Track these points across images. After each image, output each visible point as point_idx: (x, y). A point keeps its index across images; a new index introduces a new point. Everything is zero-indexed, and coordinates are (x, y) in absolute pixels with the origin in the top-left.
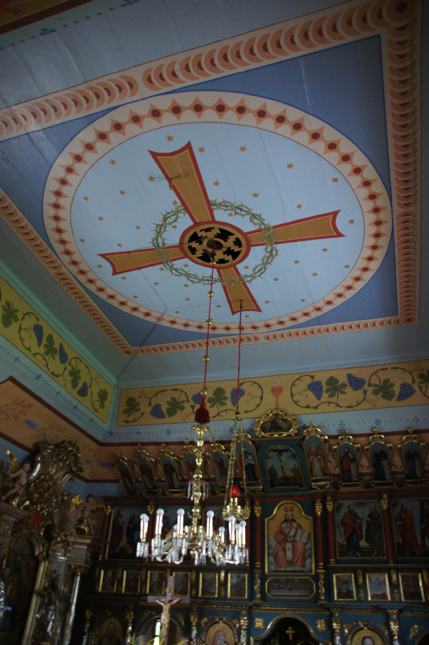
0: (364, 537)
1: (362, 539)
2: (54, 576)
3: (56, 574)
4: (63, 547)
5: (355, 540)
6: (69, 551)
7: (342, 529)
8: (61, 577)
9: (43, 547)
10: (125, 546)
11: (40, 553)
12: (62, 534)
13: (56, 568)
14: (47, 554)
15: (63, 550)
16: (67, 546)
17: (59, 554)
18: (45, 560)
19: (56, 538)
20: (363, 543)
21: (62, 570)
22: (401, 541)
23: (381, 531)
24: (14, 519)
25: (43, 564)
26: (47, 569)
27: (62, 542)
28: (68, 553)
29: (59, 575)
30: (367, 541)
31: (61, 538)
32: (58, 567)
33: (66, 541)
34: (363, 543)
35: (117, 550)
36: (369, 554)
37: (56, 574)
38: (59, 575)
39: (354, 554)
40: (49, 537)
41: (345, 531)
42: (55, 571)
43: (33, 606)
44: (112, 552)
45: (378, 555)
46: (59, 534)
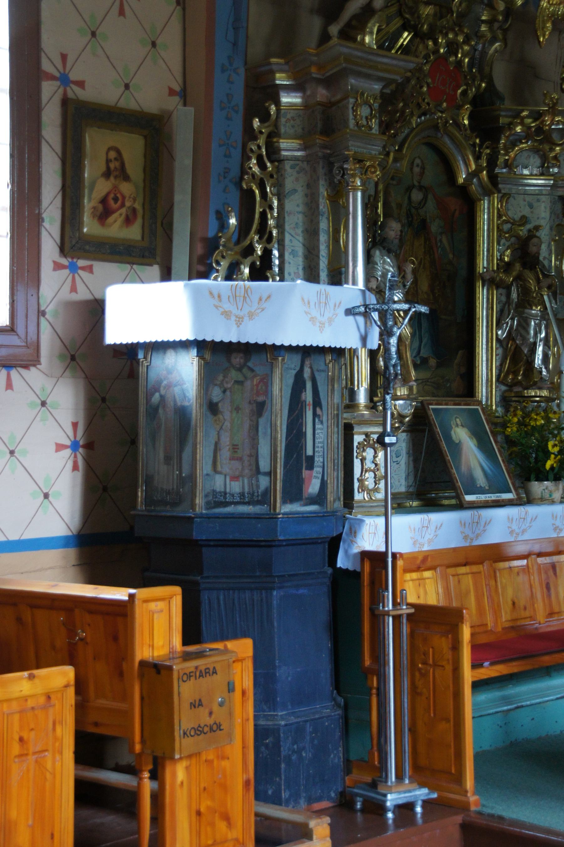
2: (523, 231)
3: (529, 226)
4: (535, 150)
6: (555, 158)
8: (544, 234)
9: (477, 158)
11: (471, 175)
12: (525, 113)
13: (526, 211)
14: (493, 178)
15: (536, 160)
16: (547, 147)
17: (526, 172)
18: (488, 193)
19: (510, 126)
21: (543, 215)
24: (377, 87)
25: (485, 204)
26: (500, 216)
27: (528, 136)
28: (553, 167)
29: (537, 228)
31: (522, 123)
32: (531, 206)
33: (539, 130)
37: (529, 226)
38: (537, 228)
40: (487, 129)
42: (524, 220)
43: (482, 312)
46: (517, 115)
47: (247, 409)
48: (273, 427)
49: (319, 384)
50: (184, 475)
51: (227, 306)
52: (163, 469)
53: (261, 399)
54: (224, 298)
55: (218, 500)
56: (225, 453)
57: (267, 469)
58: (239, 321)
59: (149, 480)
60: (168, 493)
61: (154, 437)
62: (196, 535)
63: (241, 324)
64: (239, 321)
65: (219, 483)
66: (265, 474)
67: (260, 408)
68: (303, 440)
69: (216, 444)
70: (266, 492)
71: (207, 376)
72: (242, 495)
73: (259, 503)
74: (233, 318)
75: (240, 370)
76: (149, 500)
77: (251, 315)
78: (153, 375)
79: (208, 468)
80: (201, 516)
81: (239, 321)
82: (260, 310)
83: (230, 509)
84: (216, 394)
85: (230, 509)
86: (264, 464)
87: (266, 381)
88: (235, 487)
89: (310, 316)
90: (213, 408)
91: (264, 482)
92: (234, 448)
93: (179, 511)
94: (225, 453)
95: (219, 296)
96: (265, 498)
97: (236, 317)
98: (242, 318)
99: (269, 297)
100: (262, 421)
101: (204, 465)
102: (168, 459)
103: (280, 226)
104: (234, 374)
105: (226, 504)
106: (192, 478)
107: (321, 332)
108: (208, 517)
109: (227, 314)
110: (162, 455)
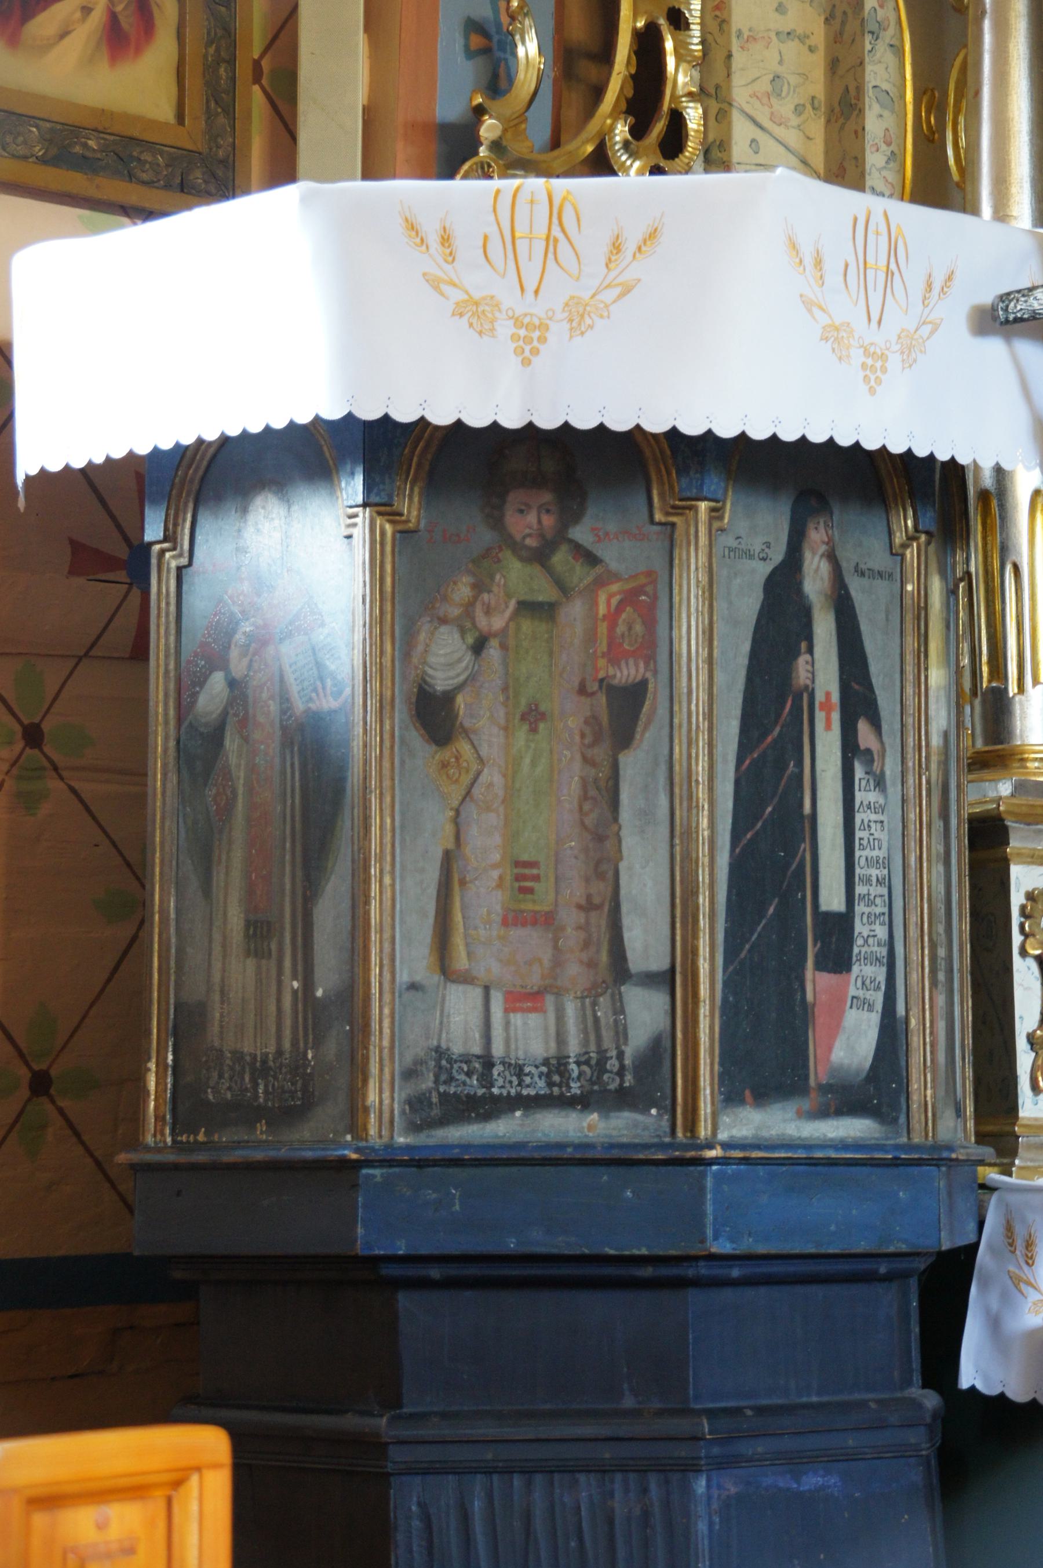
47: (571, 717)
48: (676, 784)
49: (864, 627)
50: (319, 993)
51: (477, 279)
52: (241, 973)
53: (627, 673)
54: (467, 248)
55: (462, 1088)
56: (484, 898)
57: (659, 963)
58: (530, 339)
59: (188, 1023)
60: (262, 1069)
61: (204, 850)
62: (366, 1238)
63: (535, 352)
64: (528, 340)
65: (458, 1018)
66: (650, 979)
67: (623, 711)
68: (806, 845)
69: (448, 859)
70: (658, 1056)
71: (407, 590)
72: (556, 1067)
73: (624, 1099)
74: (505, 329)
75: (540, 556)
76: (187, 1107)
77: (579, 316)
78: (200, 602)
79: (416, 960)
80: (389, 1159)
81: (530, 339)
82: (618, 291)
83: (505, 1129)
84: (445, 657)
85: (505, 1129)
86: (646, 942)
87: (648, 602)
88: (528, 1037)
89: (823, 319)
90: (434, 715)
91: (645, 1013)
92: (523, 875)
93: (303, 1141)
94: (484, 898)
95: (446, 239)
96: (654, 1078)
97: (518, 322)
98: (543, 327)
99: (652, 235)
100: (632, 765)
101: (401, 949)
102: (259, 933)
103: (713, 93)
104: (517, 576)
105: (490, 1107)
106: (352, 1001)
107: (872, 391)
108: (419, 1162)
109: (477, 313)
110: (236, 919)
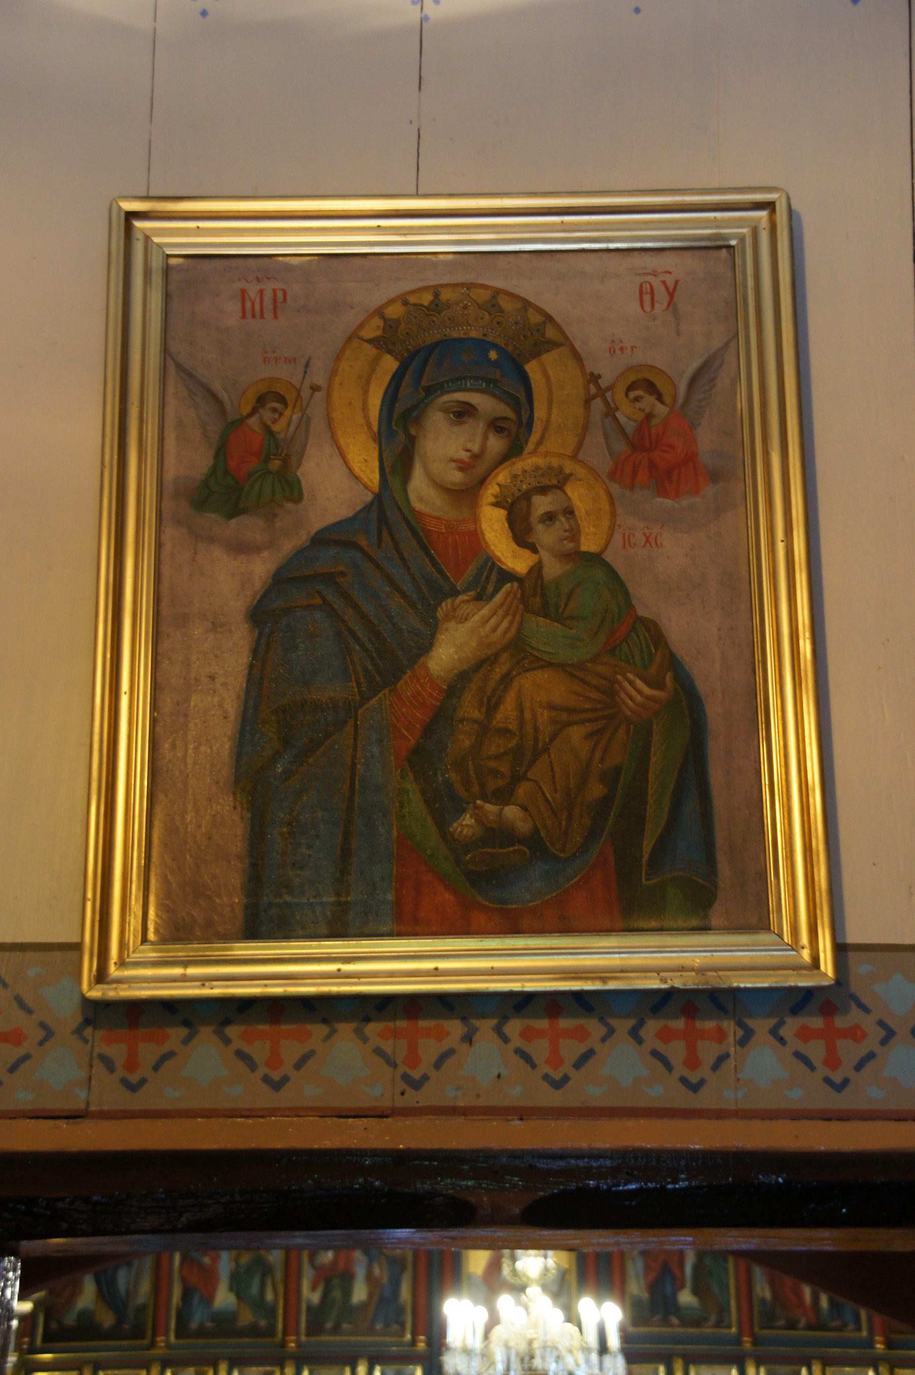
0: (689, 1283)
1: (682, 1286)
5: (669, 1288)
7: (640, 1264)
10: (92, 1306)
20: (686, 1298)
22: (768, 1294)
23: (726, 1270)
30: (695, 1292)
34: (686, 1298)
35: (70, 1319)
36: (698, 1322)
39: (666, 1322)
41: (647, 1268)
44: (54, 1325)
45: (719, 1324)
